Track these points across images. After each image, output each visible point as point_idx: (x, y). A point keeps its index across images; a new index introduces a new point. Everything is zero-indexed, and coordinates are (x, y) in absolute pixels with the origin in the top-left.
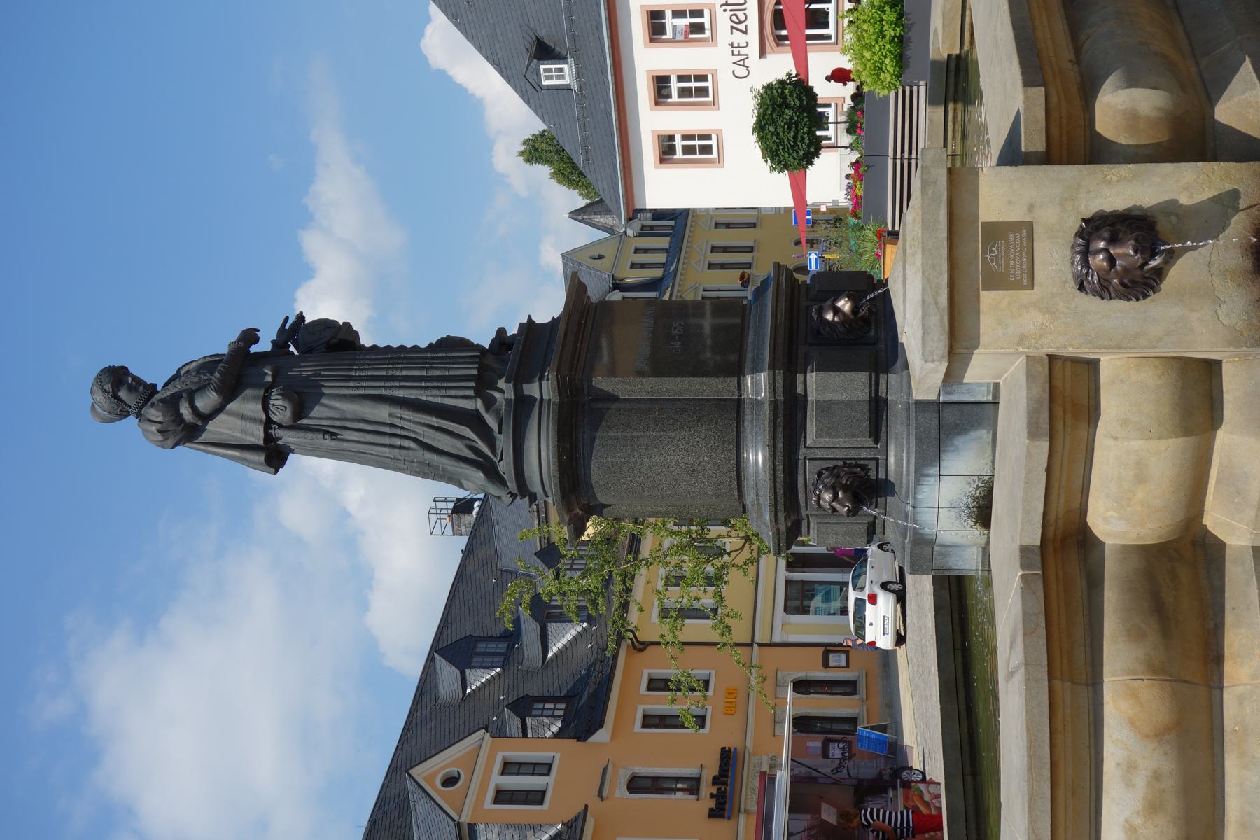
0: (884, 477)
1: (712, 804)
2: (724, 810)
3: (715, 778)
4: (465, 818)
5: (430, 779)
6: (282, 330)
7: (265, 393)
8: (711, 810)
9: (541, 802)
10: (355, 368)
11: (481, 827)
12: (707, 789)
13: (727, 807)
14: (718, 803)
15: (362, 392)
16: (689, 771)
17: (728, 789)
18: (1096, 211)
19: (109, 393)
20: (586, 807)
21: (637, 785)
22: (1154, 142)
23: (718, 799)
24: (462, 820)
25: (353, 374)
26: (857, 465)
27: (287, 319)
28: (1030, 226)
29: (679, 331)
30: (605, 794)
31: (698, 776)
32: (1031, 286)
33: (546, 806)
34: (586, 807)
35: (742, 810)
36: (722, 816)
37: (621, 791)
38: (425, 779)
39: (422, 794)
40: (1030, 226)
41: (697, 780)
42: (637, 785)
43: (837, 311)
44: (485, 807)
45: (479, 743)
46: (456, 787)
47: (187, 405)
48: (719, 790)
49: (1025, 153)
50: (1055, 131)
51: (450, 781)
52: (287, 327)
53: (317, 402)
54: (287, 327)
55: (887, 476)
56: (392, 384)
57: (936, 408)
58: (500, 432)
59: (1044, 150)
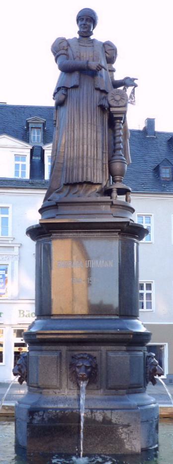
27: (137, 79)
58: (49, 200)
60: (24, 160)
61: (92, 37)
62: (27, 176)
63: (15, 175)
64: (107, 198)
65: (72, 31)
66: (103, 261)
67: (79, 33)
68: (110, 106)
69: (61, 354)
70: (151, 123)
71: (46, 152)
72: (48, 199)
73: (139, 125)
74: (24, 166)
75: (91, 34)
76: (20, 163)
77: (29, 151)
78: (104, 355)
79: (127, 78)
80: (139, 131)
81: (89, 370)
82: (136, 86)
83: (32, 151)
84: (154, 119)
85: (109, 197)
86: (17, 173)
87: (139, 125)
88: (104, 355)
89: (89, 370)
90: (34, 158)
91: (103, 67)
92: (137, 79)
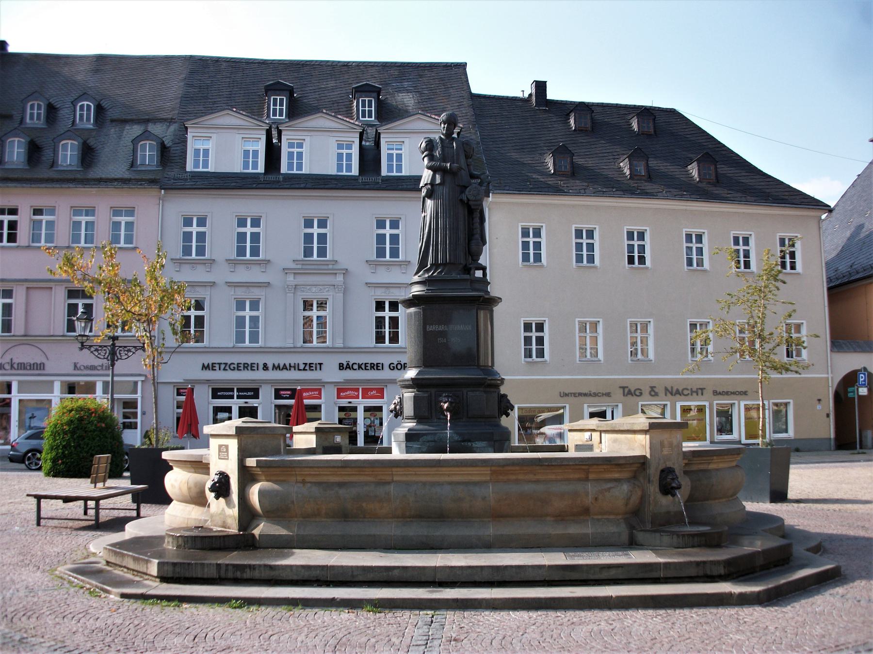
26: (401, 412)
28: (228, 459)
32: (219, 459)
40: (228, 459)
60: (349, 147)
62: (355, 171)
63: (337, 172)
64: (467, 277)
68: (468, 200)
69: (431, 394)
70: (540, 86)
71: (382, 136)
73: (523, 91)
74: (349, 156)
76: (345, 152)
78: (465, 394)
81: (454, 405)
83: (361, 135)
84: (545, 82)
85: (468, 276)
86: (340, 167)
88: (465, 394)
89: (454, 405)
90: (363, 143)
91: (463, 169)
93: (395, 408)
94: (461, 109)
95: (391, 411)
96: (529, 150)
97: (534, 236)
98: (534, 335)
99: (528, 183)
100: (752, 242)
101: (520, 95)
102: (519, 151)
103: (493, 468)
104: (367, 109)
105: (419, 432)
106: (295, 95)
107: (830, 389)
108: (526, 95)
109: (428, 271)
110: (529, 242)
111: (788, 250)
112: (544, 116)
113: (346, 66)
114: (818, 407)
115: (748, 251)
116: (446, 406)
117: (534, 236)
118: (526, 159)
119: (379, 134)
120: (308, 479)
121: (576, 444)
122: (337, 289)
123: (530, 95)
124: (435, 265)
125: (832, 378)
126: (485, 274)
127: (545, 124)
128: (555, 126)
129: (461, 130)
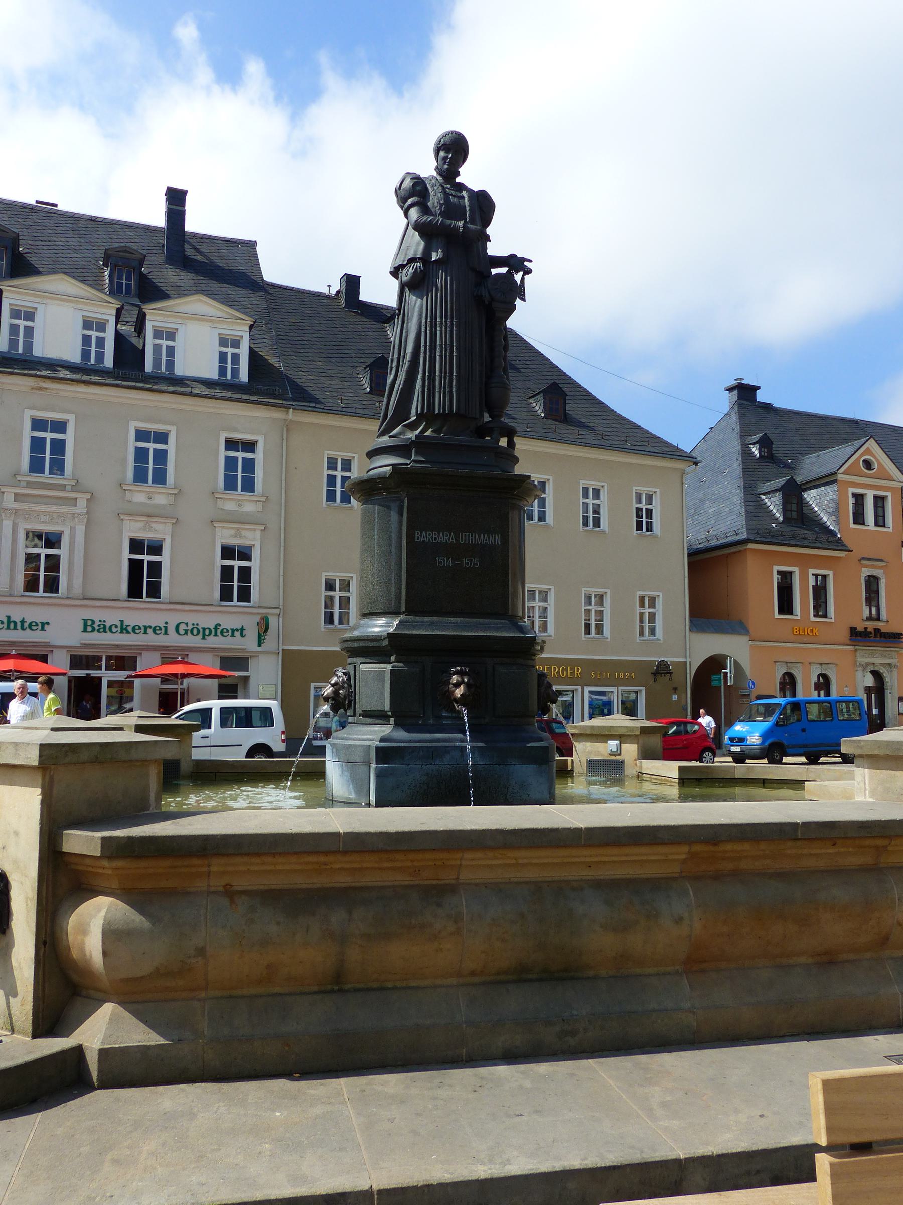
0: (349, 721)
1: (860, 628)
2: (856, 636)
3: (879, 630)
4: (840, 477)
5: (867, 451)
6: (523, 260)
7: (418, 258)
8: (855, 628)
9: (855, 522)
10: (444, 320)
11: (835, 487)
12: (871, 625)
13: (859, 638)
14: (861, 632)
15: (423, 330)
16: (884, 615)
17: (872, 638)
18: (12, 886)
19: (439, 144)
20: (852, 551)
21: (872, 584)
22: (71, 945)
23: (863, 632)
24: (839, 476)
25: (438, 320)
26: (350, 702)
27: (530, 261)
29: (468, 564)
30: (864, 562)
31: (881, 619)
33: (852, 526)
34: (852, 551)
35: (856, 647)
36: (851, 635)
37: (866, 572)
38: (868, 449)
39: (856, 448)
41: (878, 619)
42: (872, 584)
43: (457, 685)
44: (849, 488)
45: (896, 479)
46: (863, 468)
47: (415, 201)
48: (871, 632)
49: (62, 833)
50: (88, 861)
51: (868, 465)
52: (526, 263)
53: (418, 297)
54: (526, 263)
55: (349, 723)
56: (428, 351)
57: (366, 761)
59: (63, 850)
61: (458, 180)
65: (427, 168)
66: (486, 535)
67: (437, 169)
71: (147, 318)
72: (391, 434)
73: (329, 286)
75: (458, 174)
77: (114, 312)
79: (513, 256)
80: (328, 297)
82: (528, 271)
87: (329, 286)
92: (530, 261)
93: (336, 693)
94: (251, 299)
95: (326, 699)
96: (338, 360)
97: (343, 470)
98: (337, 595)
99: (339, 401)
100: (604, 494)
101: (325, 290)
102: (325, 360)
103: (697, 848)
104: (124, 281)
105: (403, 745)
106: (20, 249)
107: (688, 675)
108: (333, 292)
109: (412, 426)
110: (335, 476)
111: (644, 506)
112: (355, 320)
113: (94, 221)
114: (674, 697)
115: (599, 505)
116: (459, 692)
117: (343, 470)
118: (333, 371)
119: (145, 315)
120: (240, 883)
121: (589, 758)
122: (76, 519)
123: (338, 292)
124: (427, 416)
125: (690, 662)
126: (511, 444)
127: (358, 330)
128: (370, 333)
129: (255, 322)
